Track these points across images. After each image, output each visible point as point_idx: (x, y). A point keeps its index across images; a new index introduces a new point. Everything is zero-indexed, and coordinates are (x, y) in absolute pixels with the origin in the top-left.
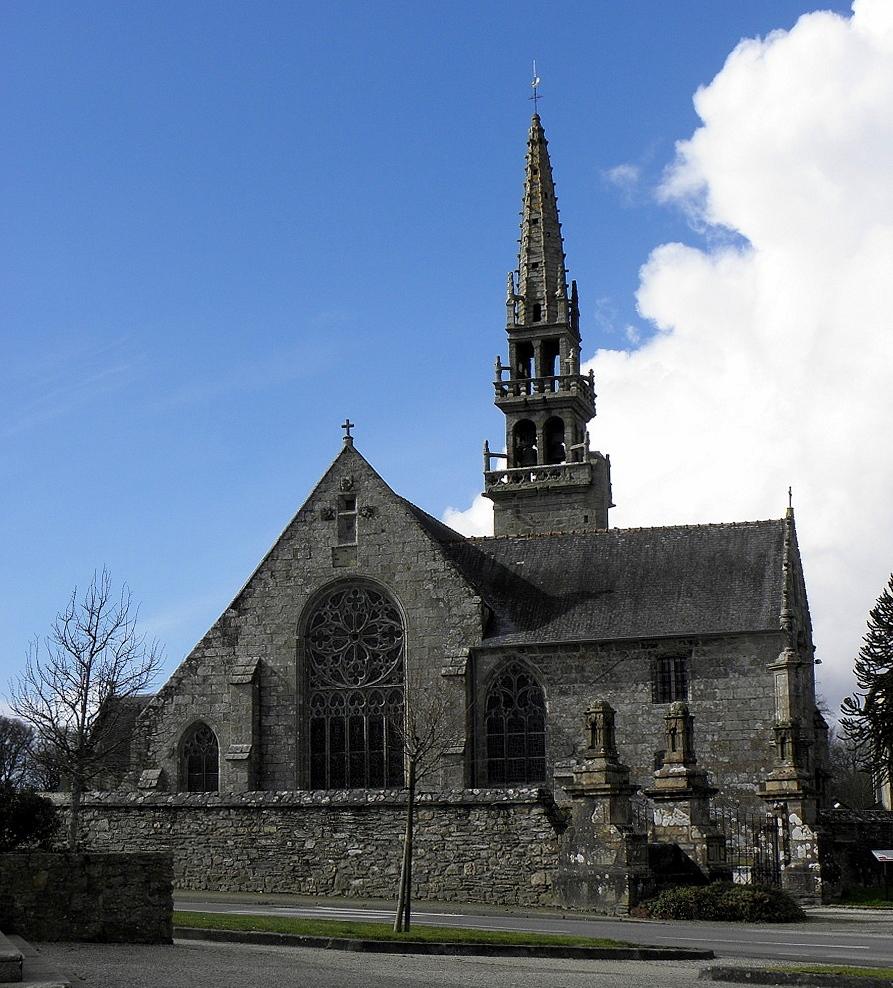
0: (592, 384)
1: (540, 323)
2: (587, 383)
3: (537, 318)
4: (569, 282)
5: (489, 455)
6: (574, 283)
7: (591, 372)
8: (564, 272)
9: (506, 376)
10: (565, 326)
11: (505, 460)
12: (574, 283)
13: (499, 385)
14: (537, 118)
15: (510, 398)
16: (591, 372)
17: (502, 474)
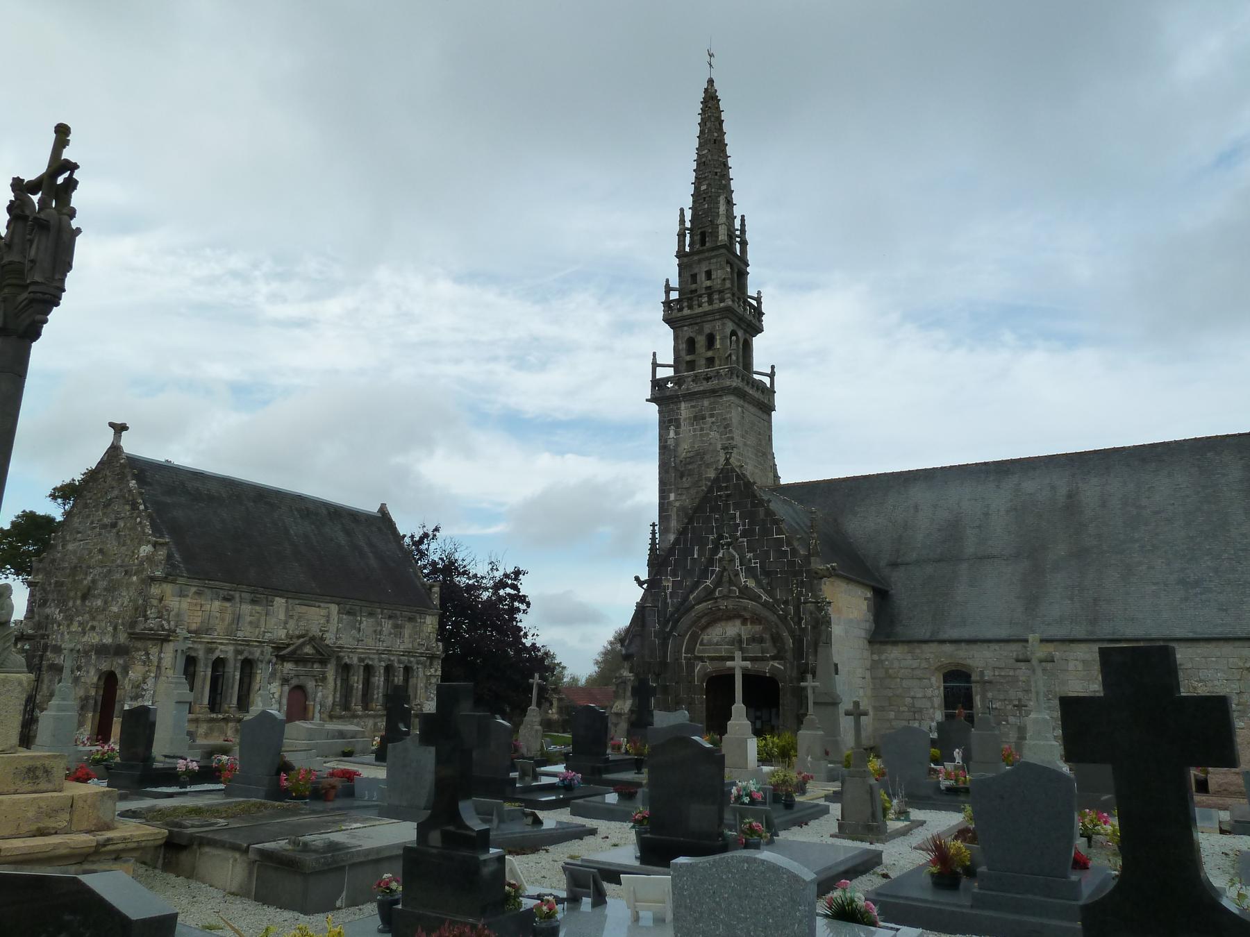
0: (759, 303)
1: (705, 248)
2: (754, 303)
3: (703, 243)
4: (737, 212)
5: (655, 365)
6: (743, 217)
7: (759, 293)
8: (730, 203)
9: (674, 295)
10: (724, 246)
11: (673, 368)
12: (743, 217)
13: (667, 304)
14: (711, 82)
15: (676, 314)
16: (759, 293)
17: (667, 380)
